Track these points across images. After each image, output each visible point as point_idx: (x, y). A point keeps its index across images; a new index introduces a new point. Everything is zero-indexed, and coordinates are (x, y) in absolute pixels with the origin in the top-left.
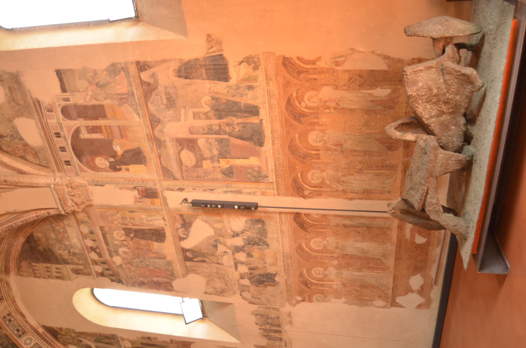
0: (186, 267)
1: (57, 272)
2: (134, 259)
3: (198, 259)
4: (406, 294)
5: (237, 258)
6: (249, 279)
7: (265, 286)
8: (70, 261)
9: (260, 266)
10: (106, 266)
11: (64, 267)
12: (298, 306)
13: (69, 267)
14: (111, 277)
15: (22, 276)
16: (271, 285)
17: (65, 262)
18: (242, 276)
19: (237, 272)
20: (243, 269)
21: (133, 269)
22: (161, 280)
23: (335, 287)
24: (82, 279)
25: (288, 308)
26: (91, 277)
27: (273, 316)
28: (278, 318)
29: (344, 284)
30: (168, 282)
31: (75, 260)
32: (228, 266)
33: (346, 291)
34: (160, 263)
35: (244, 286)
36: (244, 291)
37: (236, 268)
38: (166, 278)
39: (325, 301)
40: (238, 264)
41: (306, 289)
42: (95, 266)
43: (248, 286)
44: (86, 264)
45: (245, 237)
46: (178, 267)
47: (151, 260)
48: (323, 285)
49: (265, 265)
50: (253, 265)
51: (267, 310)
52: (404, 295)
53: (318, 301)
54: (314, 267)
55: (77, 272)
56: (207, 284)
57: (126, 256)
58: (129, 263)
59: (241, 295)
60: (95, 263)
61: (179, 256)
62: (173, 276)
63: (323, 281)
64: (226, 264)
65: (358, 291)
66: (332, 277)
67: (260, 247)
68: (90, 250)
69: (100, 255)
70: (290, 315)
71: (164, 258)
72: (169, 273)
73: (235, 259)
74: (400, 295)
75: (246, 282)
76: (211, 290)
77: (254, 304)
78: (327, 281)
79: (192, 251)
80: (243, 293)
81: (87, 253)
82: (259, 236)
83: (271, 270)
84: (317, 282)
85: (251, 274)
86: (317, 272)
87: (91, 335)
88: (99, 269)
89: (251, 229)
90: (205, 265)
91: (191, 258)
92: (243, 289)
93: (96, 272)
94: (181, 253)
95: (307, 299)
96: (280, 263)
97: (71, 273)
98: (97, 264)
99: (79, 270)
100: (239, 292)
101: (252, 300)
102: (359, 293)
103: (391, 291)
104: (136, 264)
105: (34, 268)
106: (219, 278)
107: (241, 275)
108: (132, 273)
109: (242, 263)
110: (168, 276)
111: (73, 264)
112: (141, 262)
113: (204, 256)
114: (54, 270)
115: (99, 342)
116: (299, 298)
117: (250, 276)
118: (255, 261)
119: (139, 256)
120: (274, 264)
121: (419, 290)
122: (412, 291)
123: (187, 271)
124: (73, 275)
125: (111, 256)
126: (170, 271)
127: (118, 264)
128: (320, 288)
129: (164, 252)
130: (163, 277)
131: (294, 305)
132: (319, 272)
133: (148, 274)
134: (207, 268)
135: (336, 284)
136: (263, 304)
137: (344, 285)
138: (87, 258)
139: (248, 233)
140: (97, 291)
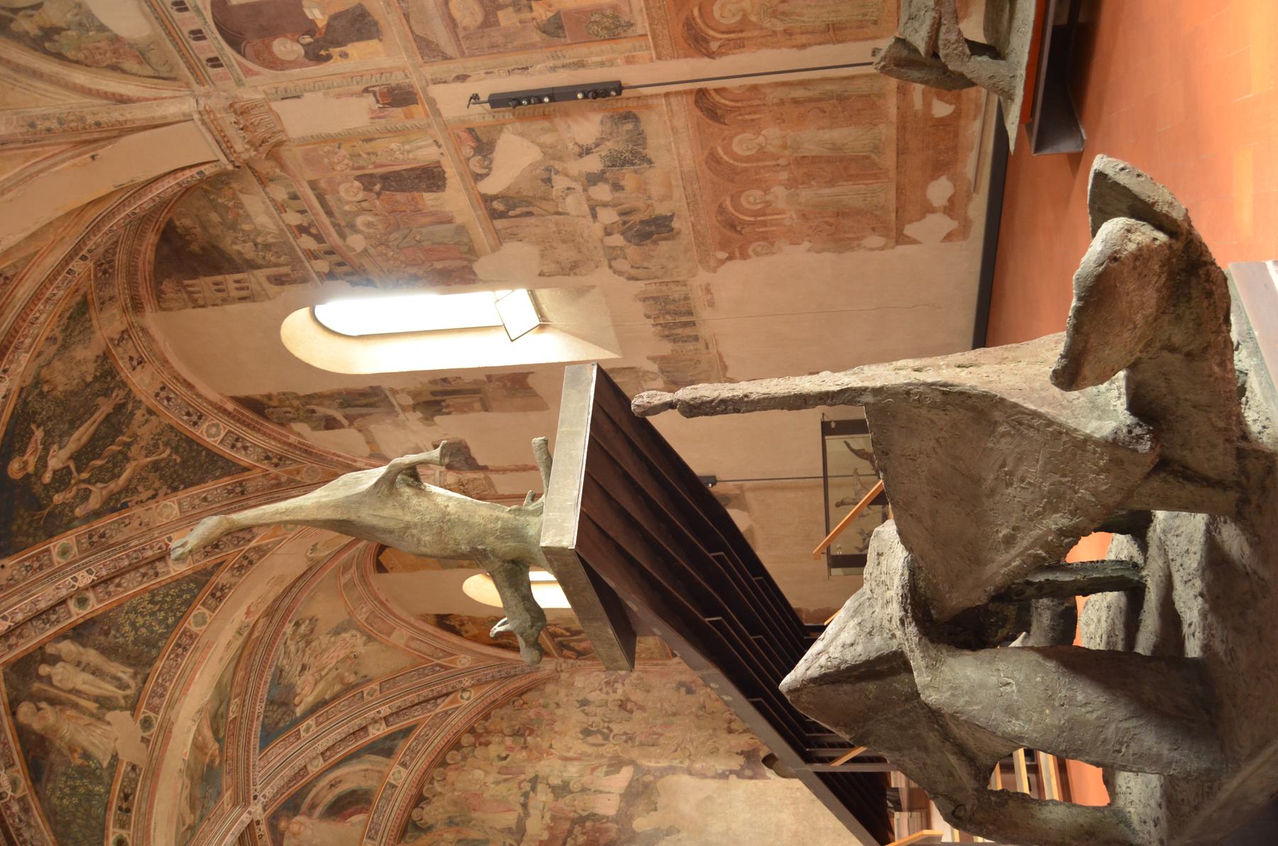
0: (496, 231)
1: (237, 289)
2: (390, 234)
3: (518, 211)
4: (923, 216)
5: (594, 197)
6: (623, 233)
7: (655, 242)
8: (260, 261)
9: (640, 204)
10: (335, 258)
11: (251, 276)
12: (722, 270)
13: (261, 274)
14: (350, 278)
15: (170, 309)
16: (665, 239)
17: (252, 265)
18: (609, 231)
19: (597, 224)
20: (608, 216)
21: (391, 253)
22: (449, 264)
23: (787, 222)
24: (290, 291)
25: (703, 276)
26: (309, 285)
27: (676, 296)
28: (686, 298)
29: (804, 215)
30: (464, 268)
31: (269, 256)
32: (578, 216)
33: (810, 227)
34: (442, 231)
35: (614, 248)
36: (615, 259)
37: (594, 216)
38: (460, 258)
39: (773, 253)
40: (597, 208)
41: (736, 236)
42: (313, 262)
43: (622, 248)
44: (294, 261)
45: (603, 154)
46: (480, 234)
47: (424, 230)
48: (764, 224)
49: (650, 202)
50: (627, 206)
51: (664, 288)
52: (919, 220)
53: (757, 254)
54: (743, 192)
55: (279, 280)
56: (543, 256)
57: (371, 231)
58: (381, 244)
59: (610, 267)
60: (313, 255)
61: (479, 212)
62: (472, 253)
63: (764, 215)
64: (573, 212)
65: (831, 225)
66: (781, 204)
67: (636, 167)
68: (297, 232)
69: (319, 238)
70: (708, 290)
71: (450, 221)
72: (465, 249)
73: (589, 199)
74: (911, 222)
75: (617, 240)
76: (551, 267)
77: (637, 279)
78: (772, 214)
79: (503, 197)
80: (613, 263)
81: (292, 240)
82: (630, 146)
83: (662, 209)
84: (752, 219)
85: (624, 223)
86: (752, 199)
87: (331, 396)
88: (323, 265)
89: (614, 135)
90: (532, 220)
91: (502, 212)
92: (612, 255)
93: (318, 274)
94: (482, 205)
95: (737, 254)
96: (678, 193)
97: (267, 285)
98: (316, 258)
99: (282, 275)
100: (606, 263)
101: (633, 272)
102: (834, 227)
103: (893, 215)
104: (396, 243)
105: (191, 289)
106: (564, 242)
107: (606, 228)
108: (391, 262)
109: (605, 205)
110: (464, 256)
111: (267, 267)
112: (404, 238)
113: (529, 204)
114: (232, 286)
115: (349, 406)
116: (722, 255)
117: (622, 228)
118: (629, 197)
119: (399, 226)
120: (667, 197)
121: (945, 207)
122: (932, 210)
123: (500, 239)
124: (272, 289)
125: (343, 236)
126: (466, 244)
127: (359, 249)
128: (761, 230)
129: (447, 210)
130: (453, 259)
131: (714, 270)
132: (755, 199)
133: (423, 258)
134: (537, 226)
135: (790, 217)
136: (656, 277)
137: (804, 216)
138: (293, 249)
139: (609, 144)
140: (320, 310)
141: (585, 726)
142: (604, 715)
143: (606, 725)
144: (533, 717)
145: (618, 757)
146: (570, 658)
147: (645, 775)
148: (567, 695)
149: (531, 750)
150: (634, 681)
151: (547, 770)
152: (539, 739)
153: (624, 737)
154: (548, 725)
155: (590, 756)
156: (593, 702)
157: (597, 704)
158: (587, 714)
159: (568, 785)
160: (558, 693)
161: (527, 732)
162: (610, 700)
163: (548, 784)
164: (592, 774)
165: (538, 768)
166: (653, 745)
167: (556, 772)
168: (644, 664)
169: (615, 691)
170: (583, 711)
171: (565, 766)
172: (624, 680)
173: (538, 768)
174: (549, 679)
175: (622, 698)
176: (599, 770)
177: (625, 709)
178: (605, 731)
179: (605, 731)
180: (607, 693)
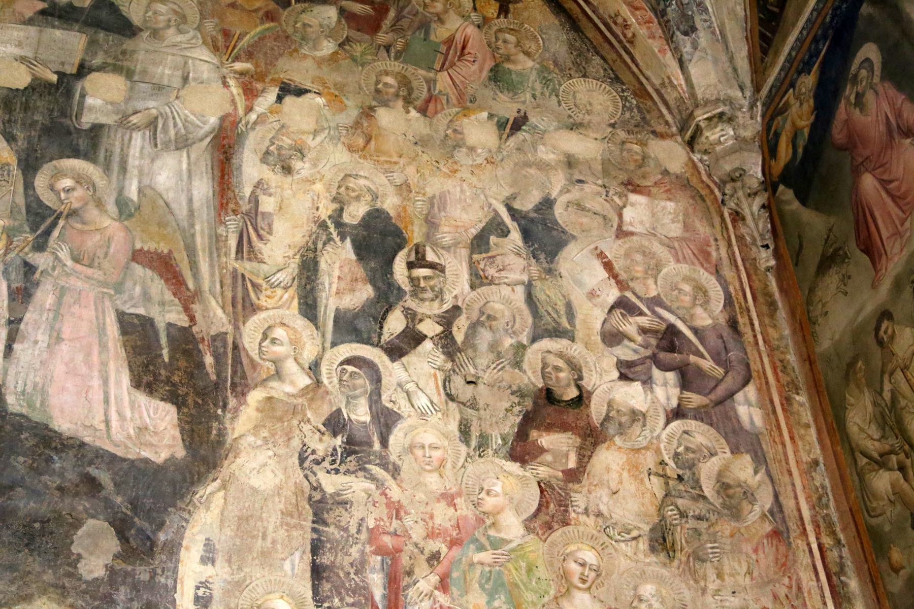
141: (416, 234)
142: (484, 320)
143: (430, 328)
144: (440, 33)
145: (241, 388)
146: (770, 149)
147: (122, 528)
148: (570, 162)
149: (270, 16)
150: (708, 470)
151: (165, 72)
152: (328, 47)
153: (361, 414)
154: (405, 82)
155: (245, 249)
156: (550, 271)
157: (545, 291)
158: (480, 243)
159: (89, 155)
160: (574, 126)
161: (358, 8)
162: (576, 350)
163: (83, 70)
164: (137, 256)
165: (172, 36)
166: (317, 572)
167: (153, 105)
168: (823, 525)
169: (626, 372)
170: (496, 227)
171: (182, 143)
172: (700, 414)
173: (172, 36)
174: (641, 93)
175: (596, 410)
176: (158, 287)
177: (529, 421)
178: (395, 324)
179: (395, 324)
180: (612, 338)
